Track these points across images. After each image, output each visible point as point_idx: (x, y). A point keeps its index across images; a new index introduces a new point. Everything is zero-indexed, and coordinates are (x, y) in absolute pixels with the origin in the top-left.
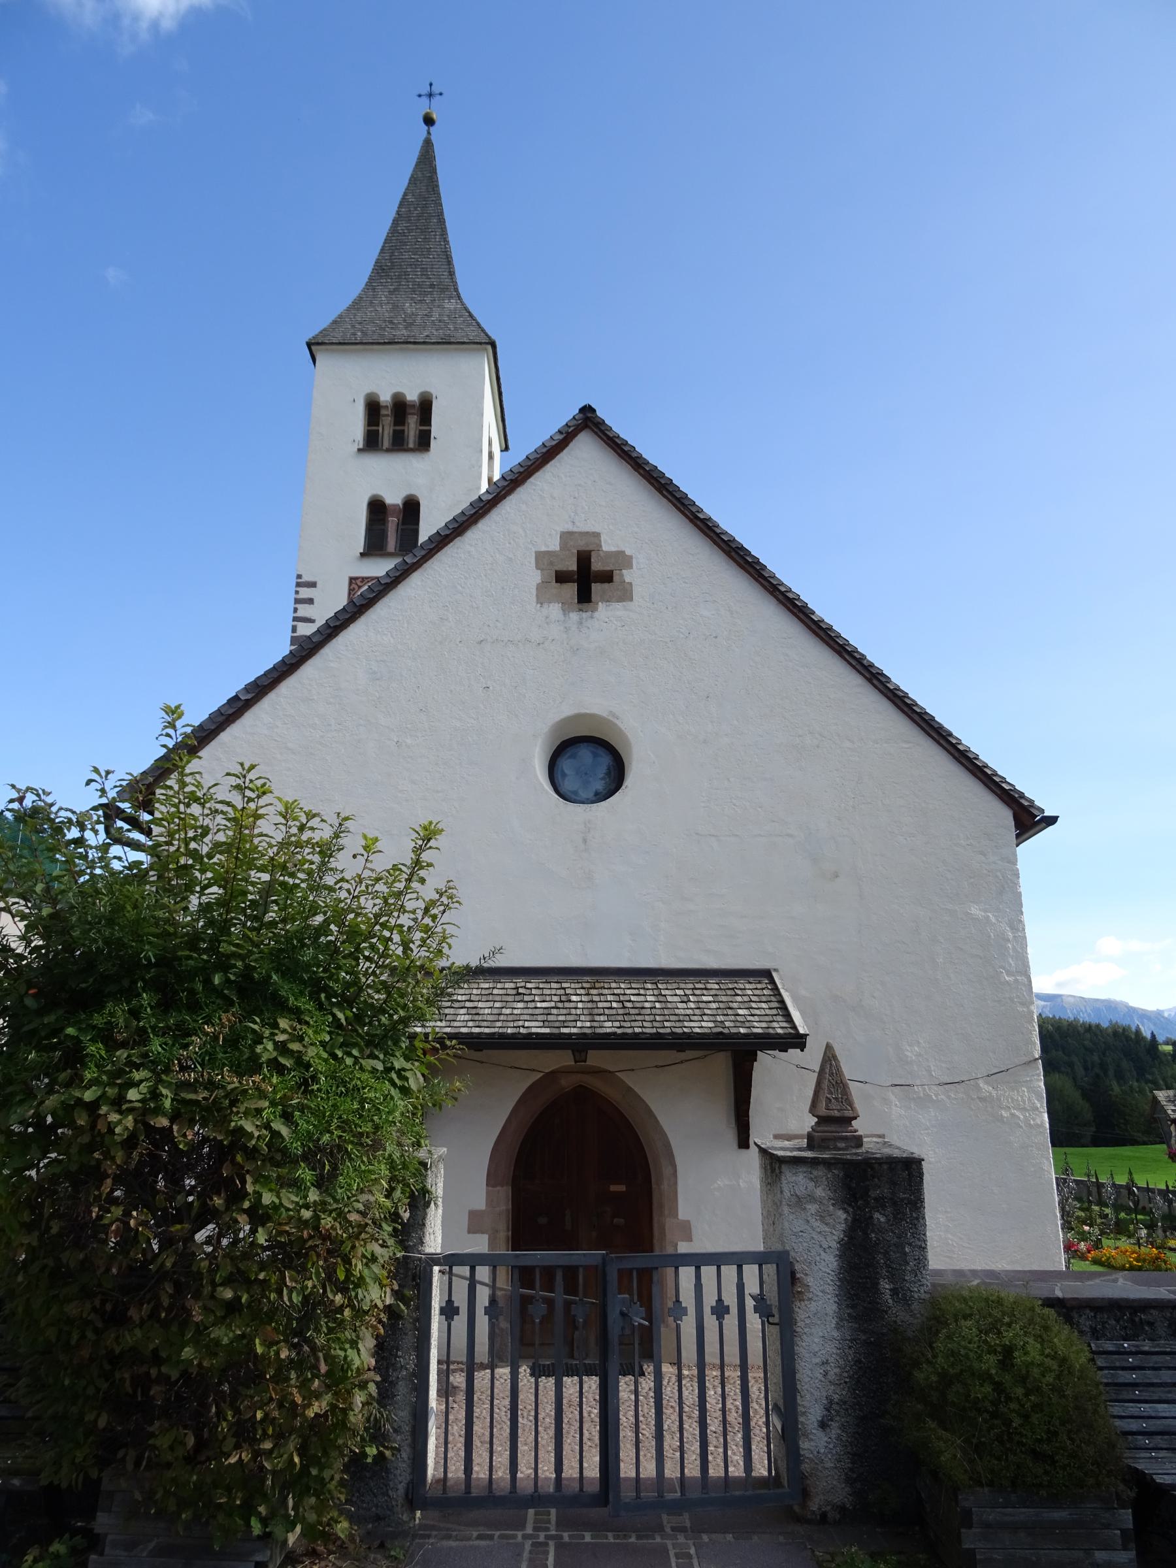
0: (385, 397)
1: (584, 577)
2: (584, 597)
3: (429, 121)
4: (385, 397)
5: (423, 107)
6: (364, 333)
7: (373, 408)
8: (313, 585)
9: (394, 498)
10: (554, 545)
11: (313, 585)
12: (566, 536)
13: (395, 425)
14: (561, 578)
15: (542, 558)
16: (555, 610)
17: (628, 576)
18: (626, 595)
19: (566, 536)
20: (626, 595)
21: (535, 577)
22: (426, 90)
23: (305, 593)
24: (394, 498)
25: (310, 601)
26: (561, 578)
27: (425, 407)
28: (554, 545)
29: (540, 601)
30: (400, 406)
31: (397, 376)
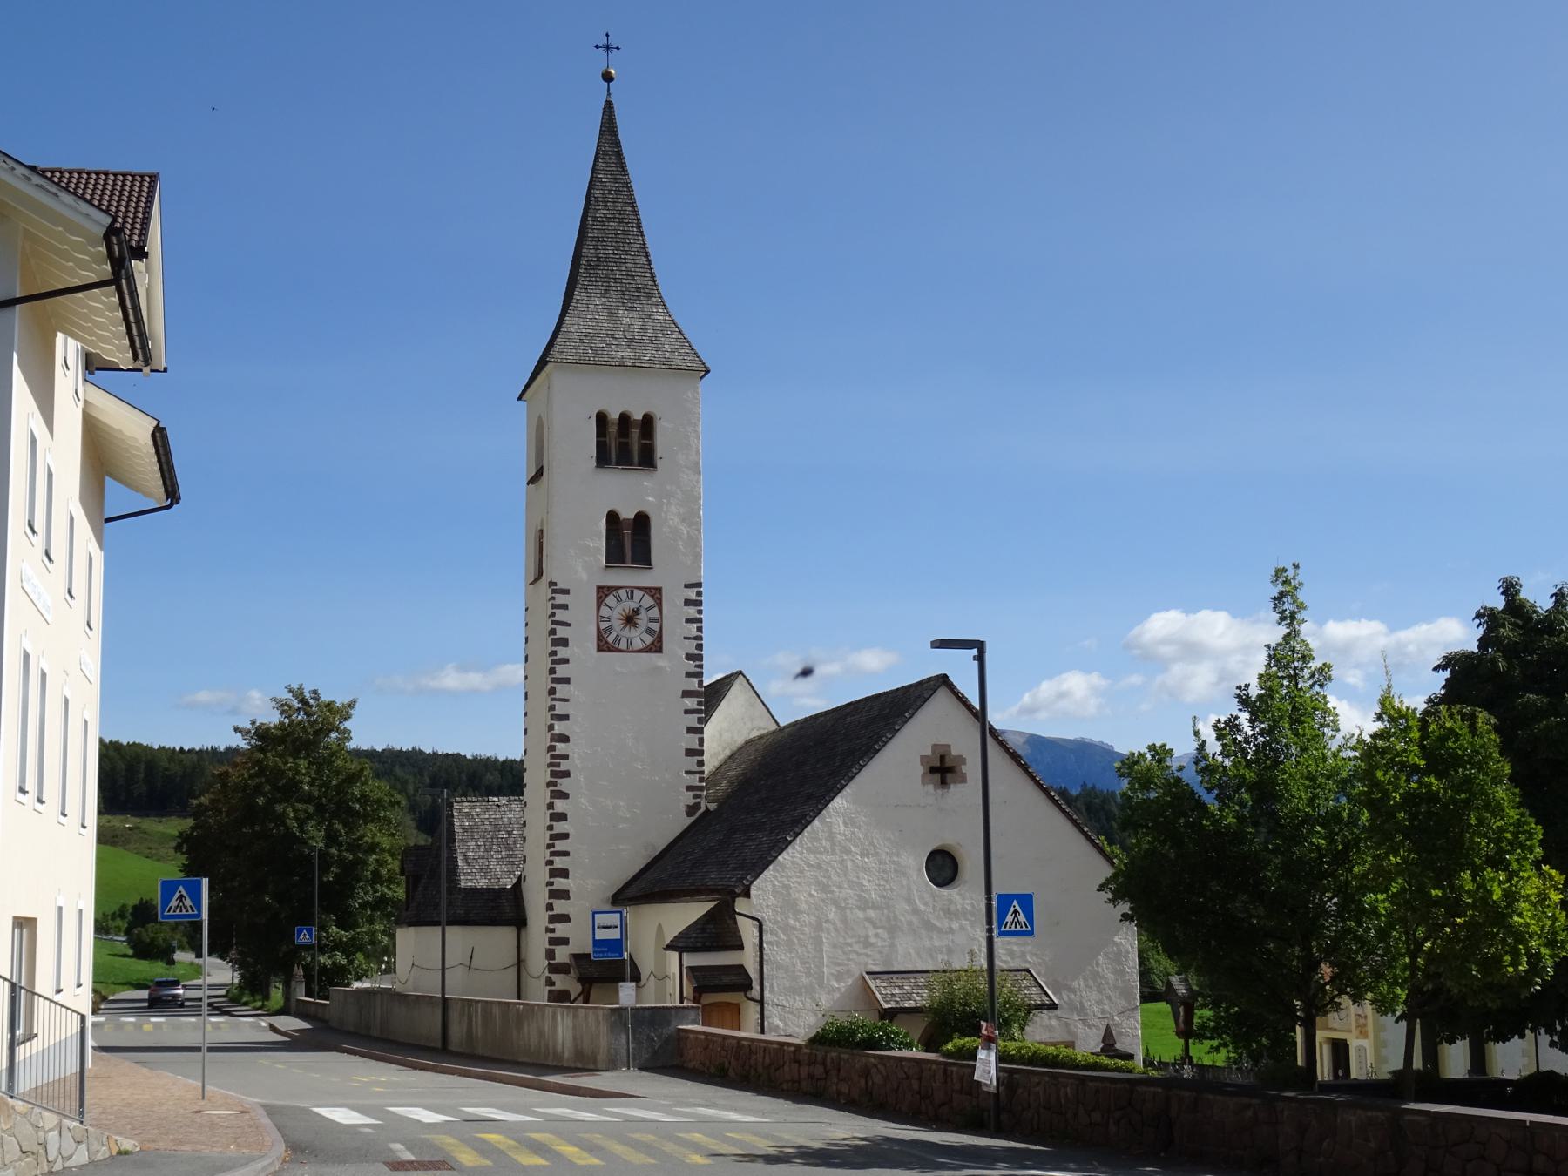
0: (614, 415)
1: (942, 770)
2: (944, 783)
3: (608, 77)
4: (614, 415)
5: (599, 61)
6: (595, 352)
7: (602, 419)
8: (566, 592)
9: (627, 514)
10: (929, 753)
11: (566, 592)
12: (935, 746)
13: (627, 444)
14: (933, 770)
15: (922, 758)
16: (930, 787)
17: (964, 769)
18: (964, 780)
19: (935, 746)
20: (964, 780)
21: (920, 770)
22: (603, 42)
23: (560, 599)
24: (627, 514)
25: (565, 607)
26: (933, 770)
27: (648, 422)
28: (929, 753)
29: (924, 783)
30: (624, 418)
31: (626, 397)
